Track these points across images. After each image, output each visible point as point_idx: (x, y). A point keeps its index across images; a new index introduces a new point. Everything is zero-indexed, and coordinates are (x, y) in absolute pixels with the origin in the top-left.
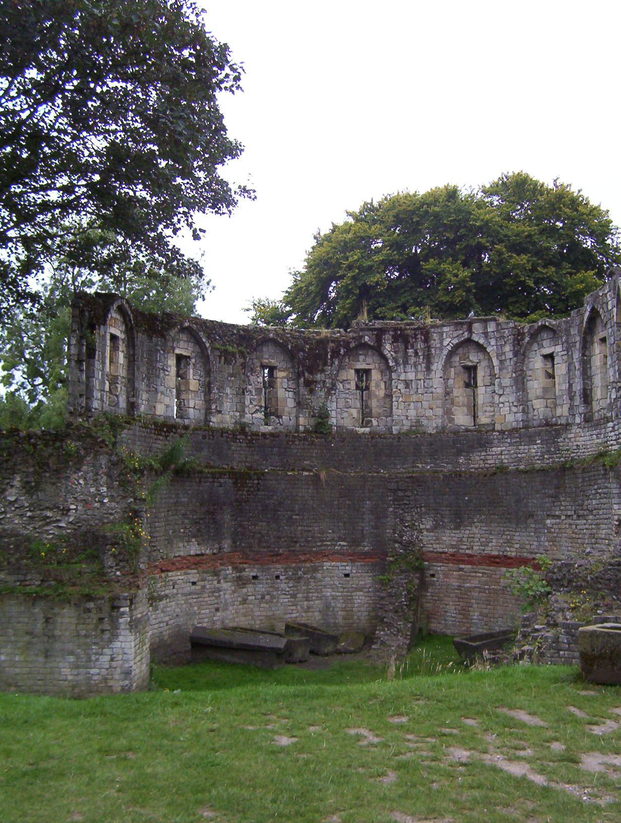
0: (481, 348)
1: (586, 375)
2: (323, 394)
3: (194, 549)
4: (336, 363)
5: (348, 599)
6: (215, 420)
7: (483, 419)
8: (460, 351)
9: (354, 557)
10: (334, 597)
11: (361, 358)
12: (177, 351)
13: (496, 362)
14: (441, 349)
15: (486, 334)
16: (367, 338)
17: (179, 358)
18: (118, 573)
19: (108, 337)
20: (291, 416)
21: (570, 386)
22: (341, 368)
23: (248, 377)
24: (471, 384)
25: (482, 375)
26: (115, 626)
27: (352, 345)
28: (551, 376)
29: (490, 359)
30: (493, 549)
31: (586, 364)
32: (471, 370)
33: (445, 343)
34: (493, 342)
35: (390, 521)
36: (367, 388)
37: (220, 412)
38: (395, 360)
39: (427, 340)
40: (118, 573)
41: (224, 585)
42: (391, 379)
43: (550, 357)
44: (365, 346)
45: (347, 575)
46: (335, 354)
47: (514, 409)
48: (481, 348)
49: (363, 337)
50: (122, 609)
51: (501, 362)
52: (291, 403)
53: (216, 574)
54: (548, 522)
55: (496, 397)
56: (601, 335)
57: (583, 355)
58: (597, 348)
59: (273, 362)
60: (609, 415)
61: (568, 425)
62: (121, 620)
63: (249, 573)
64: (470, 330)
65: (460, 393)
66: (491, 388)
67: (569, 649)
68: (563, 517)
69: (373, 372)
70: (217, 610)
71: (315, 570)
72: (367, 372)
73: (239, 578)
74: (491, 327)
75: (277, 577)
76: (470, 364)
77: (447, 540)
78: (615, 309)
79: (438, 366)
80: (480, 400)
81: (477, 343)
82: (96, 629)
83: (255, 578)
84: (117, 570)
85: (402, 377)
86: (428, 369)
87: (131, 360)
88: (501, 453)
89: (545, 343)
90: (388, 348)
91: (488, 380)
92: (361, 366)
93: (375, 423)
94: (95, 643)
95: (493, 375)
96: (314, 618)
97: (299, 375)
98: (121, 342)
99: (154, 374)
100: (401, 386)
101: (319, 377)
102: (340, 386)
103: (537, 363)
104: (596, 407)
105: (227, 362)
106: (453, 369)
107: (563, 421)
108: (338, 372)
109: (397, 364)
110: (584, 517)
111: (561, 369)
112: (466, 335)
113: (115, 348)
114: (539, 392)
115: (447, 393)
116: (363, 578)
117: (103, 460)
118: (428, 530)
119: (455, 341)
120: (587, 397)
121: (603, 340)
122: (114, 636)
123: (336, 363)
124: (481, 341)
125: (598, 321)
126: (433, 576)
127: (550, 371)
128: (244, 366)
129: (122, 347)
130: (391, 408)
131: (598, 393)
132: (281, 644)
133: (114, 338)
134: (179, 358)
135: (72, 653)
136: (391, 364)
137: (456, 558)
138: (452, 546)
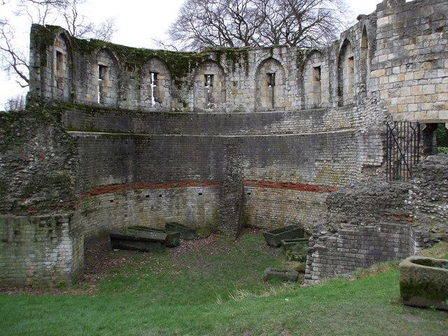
0: (278, 63)
2: (185, 89)
3: (111, 180)
4: (194, 71)
5: (201, 207)
6: (123, 105)
8: (265, 64)
9: (205, 183)
10: (193, 207)
11: (208, 68)
12: (99, 63)
15: (281, 55)
16: (211, 57)
17: (101, 67)
18: (61, 201)
19: (55, 53)
20: (168, 103)
21: (330, 85)
22: (196, 74)
23: (142, 79)
24: (271, 82)
26: (60, 235)
27: (203, 60)
28: (318, 80)
31: (340, 72)
32: (271, 76)
33: (257, 60)
34: (285, 59)
35: (225, 163)
37: (125, 100)
38: (228, 70)
39: (246, 58)
40: (61, 201)
41: (130, 202)
42: (225, 81)
43: (319, 68)
44: (210, 61)
45: (200, 194)
46: (193, 66)
47: (296, 98)
48: (278, 63)
49: (209, 55)
50: (63, 224)
51: (290, 71)
52: (167, 94)
53: (125, 195)
54: (316, 164)
55: (286, 91)
56: (350, 56)
57: (339, 67)
58: (346, 64)
59: (157, 70)
62: (63, 231)
63: (145, 193)
64: (272, 53)
66: (284, 86)
67: (343, 247)
68: (325, 161)
70: (126, 216)
71: (182, 191)
72: (212, 76)
73: (138, 197)
75: (161, 196)
76: (271, 72)
78: (361, 40)
79: (252, 73)
80: (276, 93)
82: (48, 236)
83: (148, 196)
84: (61, 199)
85: (232, 80)
86: (247, 75)
87: (71, 68)
88: (288, 124)
89: (316, 60)
90: (223, 62)
91: (281, 82)
93: (216, 106)
94: (47, 246)
95: (284, 80)
96: (181, 219)
97: (172, 78)
98: (64, 57)
99: (84, 76)
100: (232, 85)
101: (183, 79)
102: (196, 84)
103: (309, 73)
104: (345, 97)
105: (130, 69)
106: (261, 75)
107: (325, 106)
108: (195, 76)
109: (229, 71)
110: (338, 161)
112: (269, 55)
113: (60, 60)
116: (209, 194)
117: (50, 129)
118: (247, 168)
119: (263, 59)
120: (340, 92)
121: (352, 58)
122: (60, 241)
123: (194, 71)
124: (278, 59)
125: (349, 47)
126: (249, 194)
127: (318, 77)
128: (139, 72)
129: (64, 59)
130: (225, 97)
131: (346, 89)
132: (163, 237)
133: (59, 54)
134: (101, 67)
135: (33, 253)
136: (225, 72)
137: (263, 184)
138: (261, 177)
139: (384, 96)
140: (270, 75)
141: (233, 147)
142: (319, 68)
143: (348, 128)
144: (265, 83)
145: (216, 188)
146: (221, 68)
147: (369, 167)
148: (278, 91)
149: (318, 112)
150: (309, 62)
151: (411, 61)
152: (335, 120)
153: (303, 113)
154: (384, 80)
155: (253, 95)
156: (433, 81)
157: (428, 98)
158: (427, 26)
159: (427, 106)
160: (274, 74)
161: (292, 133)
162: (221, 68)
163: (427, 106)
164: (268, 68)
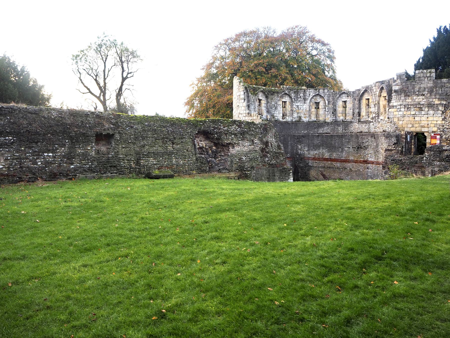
1: (360, 108)
7: (321, 119)
8: (314, 97)
13: (327, 102)
14: (309, 97)
24: (317, 108)
25: (321, 105)
30: (327, 155)
32: (317, 104)
36: (285, 107)
43: (345, 102)
44: (286, 94)
51: (329, 102)
58: (364, 102)
59: (260, 98)
60: (372, 121)
61: (351, 122)
64: (319, 91)
65: (313, 110)
69: (287, 102)
72: (285, 102)
74: (326, 91)
77: (313, 153)
79: (308, 101)
81: (321, 96)
88: (326, 130)
91: (323, 107)
92: (284, 100)
93: (287, 117)
103: (340, 103)
107: (349, 120)
111: (349, 105)
112: (317, 93)
114: (341, 112)
115: (309, 110)
118: (306, 151)
119: (314, 95)
120: (359, 114)
127: (344, 106)
131: (363, 113)
137: (314, 159)
139: (396, 120)
140: (316, 103)
141: (299, 139)
142: (345, 102)
143: (367, 132)
144: (314, 107)
145: (291, 161)
146: (290, 97)
147: (389, 150)
148: (321, 112)
149: (346, 124)
150: (340, 98)
151: (409, 106)
152: (356, 127)
153: (336, 123)
154: (397, 113)
155: (308, 113)
156: (420, 115)
157: (417, 122)
158: (417, 93)
159: (417, 125)
160: (319, 103)
161: (330, 133)
162: (290, 97)
163: (417, 125)
164: (315, 99)
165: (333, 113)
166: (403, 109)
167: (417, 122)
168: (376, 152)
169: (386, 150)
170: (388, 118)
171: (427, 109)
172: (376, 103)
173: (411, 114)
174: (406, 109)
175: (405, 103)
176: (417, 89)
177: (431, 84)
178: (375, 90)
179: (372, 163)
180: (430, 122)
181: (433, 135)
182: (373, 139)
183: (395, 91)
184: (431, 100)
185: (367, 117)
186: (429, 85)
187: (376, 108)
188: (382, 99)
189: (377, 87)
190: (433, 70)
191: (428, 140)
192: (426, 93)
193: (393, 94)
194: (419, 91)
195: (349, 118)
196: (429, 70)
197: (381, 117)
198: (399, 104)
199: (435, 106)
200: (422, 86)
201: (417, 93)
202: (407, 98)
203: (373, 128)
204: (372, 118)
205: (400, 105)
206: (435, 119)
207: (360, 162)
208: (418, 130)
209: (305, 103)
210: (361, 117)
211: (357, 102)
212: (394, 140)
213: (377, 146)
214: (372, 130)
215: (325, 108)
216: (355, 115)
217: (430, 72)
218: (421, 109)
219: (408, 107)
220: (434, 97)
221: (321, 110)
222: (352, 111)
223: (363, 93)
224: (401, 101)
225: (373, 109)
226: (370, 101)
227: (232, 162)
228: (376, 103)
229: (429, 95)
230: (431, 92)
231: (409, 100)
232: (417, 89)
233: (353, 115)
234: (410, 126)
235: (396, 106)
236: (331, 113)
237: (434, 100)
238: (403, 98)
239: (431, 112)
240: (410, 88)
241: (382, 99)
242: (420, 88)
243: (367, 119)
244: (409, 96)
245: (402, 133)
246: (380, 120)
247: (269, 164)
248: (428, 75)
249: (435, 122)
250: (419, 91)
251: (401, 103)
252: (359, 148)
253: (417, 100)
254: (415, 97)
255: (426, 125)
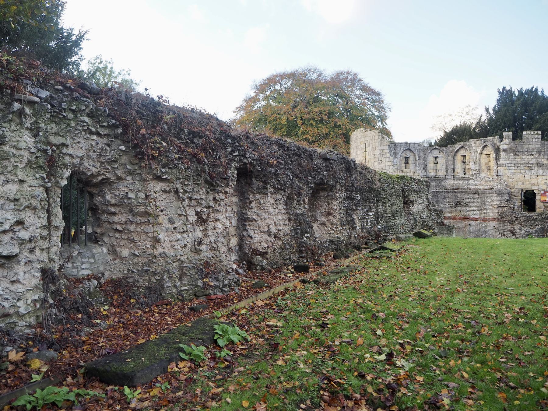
1: (454, 164)
25: (411, 161)
29: (415, 155)
32: (407, 158)
43: (436, 158)
51: (419, 157)
58: (459, 158)
81: (411, 150)
91: (413, 162)
107: (441, 177)
111: (442, 161)
114: (432, 168)
139: (505, 178)
140: (406, 158)
142: (436, 158)
147: (501, 207)
149: (439, 180)
152: (450, 184)
154: (507, 171)
157: (527, 180)
158: (526, 153)
163: (527, 183)
165: (424, 169)
166: (513, 168)
167: (527, 180)
168: (482, 208)
169: (498, 207)
170: (497, 176)
171: (536, 168)
172: (477, 160)
173: (521, 173)
174: (516, 168)
175: (514, 162)
176: (525, 149)
177: (538, 145)
178: (474, 148)
179: (476, 219)
180: (539, 181)
181: (543, 192)
182: (476, 196)
183: (504, 150)
184: (540, 160)
185: (463, 173)
186: (537, 146)
187: (478, 165)
188: (484, 156)
189: (477, 145)
190: (540, 132)
191: (538, 197)
192: (534, 153)
193: (502, 153)
194: (527, 151)
195: (441, 174)
196: (536, 132)
197: (483, 175)
198: (508, 162)
199: (545, 165)
200: (530, 146)
201: (526, 153)
202: (517, 157)
203: (482, 186)
204: (473, 175)
205: (510, 164)
206: (544, 177)
207: (460, 219)
208: (528, 187)
209: (395, 157)
210: (456, 173)
211: (450, 158)
212: (506, 197)
213: (483, 202)
214: (473, 187)
215: (416, 164)
216: (449, 172)
217: (537, 134)
218: (530, 168)
219: (517, 166)
220: (542, 157)
221: (411, 165)
222: (445, 167)
223: (458, 150)
224: (510, 159)
225: (472, 166)
226: (467, 158)
227: (415, 220)
228: (477, 160)
229: (538, 155)
230: (540, 152)
231: (518, 159)
232: (525, 149)
233: (447, 171)
234: (521, 183)
235: (506, 165)
236: (422, 169)
237: (543, 160)
238: (512, 157)
239: (541, 171)
240: (518, 148)
241: (484, 156)
242: (528, 148)
243: (464, 176)
244: (518, 155)
245: (512, 190)
246: (482, 178)
247: (437, 222)
248: (536, 136)
249: (545, 181)
250: (527, 151)
251: (511, 162)
252: (458, 204)
253: (526, 160)
254: (524, 157)
255: (536, 183)
